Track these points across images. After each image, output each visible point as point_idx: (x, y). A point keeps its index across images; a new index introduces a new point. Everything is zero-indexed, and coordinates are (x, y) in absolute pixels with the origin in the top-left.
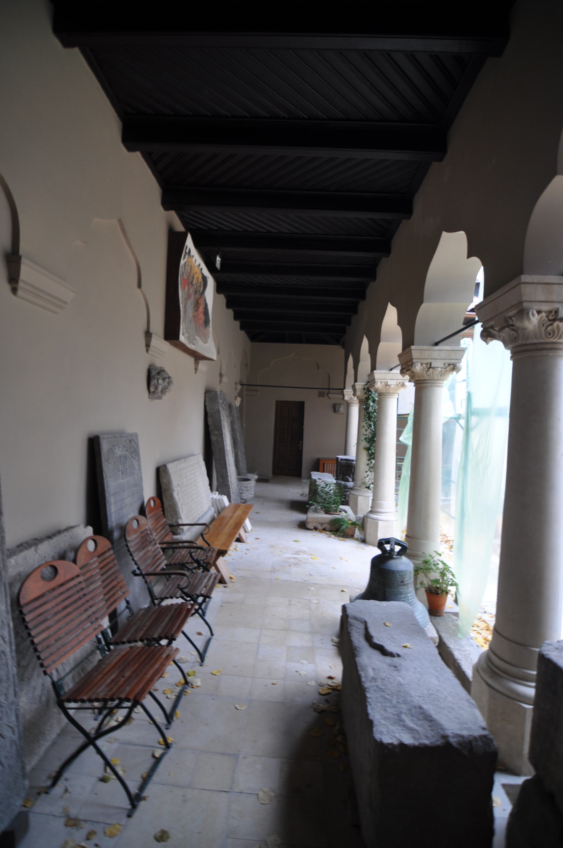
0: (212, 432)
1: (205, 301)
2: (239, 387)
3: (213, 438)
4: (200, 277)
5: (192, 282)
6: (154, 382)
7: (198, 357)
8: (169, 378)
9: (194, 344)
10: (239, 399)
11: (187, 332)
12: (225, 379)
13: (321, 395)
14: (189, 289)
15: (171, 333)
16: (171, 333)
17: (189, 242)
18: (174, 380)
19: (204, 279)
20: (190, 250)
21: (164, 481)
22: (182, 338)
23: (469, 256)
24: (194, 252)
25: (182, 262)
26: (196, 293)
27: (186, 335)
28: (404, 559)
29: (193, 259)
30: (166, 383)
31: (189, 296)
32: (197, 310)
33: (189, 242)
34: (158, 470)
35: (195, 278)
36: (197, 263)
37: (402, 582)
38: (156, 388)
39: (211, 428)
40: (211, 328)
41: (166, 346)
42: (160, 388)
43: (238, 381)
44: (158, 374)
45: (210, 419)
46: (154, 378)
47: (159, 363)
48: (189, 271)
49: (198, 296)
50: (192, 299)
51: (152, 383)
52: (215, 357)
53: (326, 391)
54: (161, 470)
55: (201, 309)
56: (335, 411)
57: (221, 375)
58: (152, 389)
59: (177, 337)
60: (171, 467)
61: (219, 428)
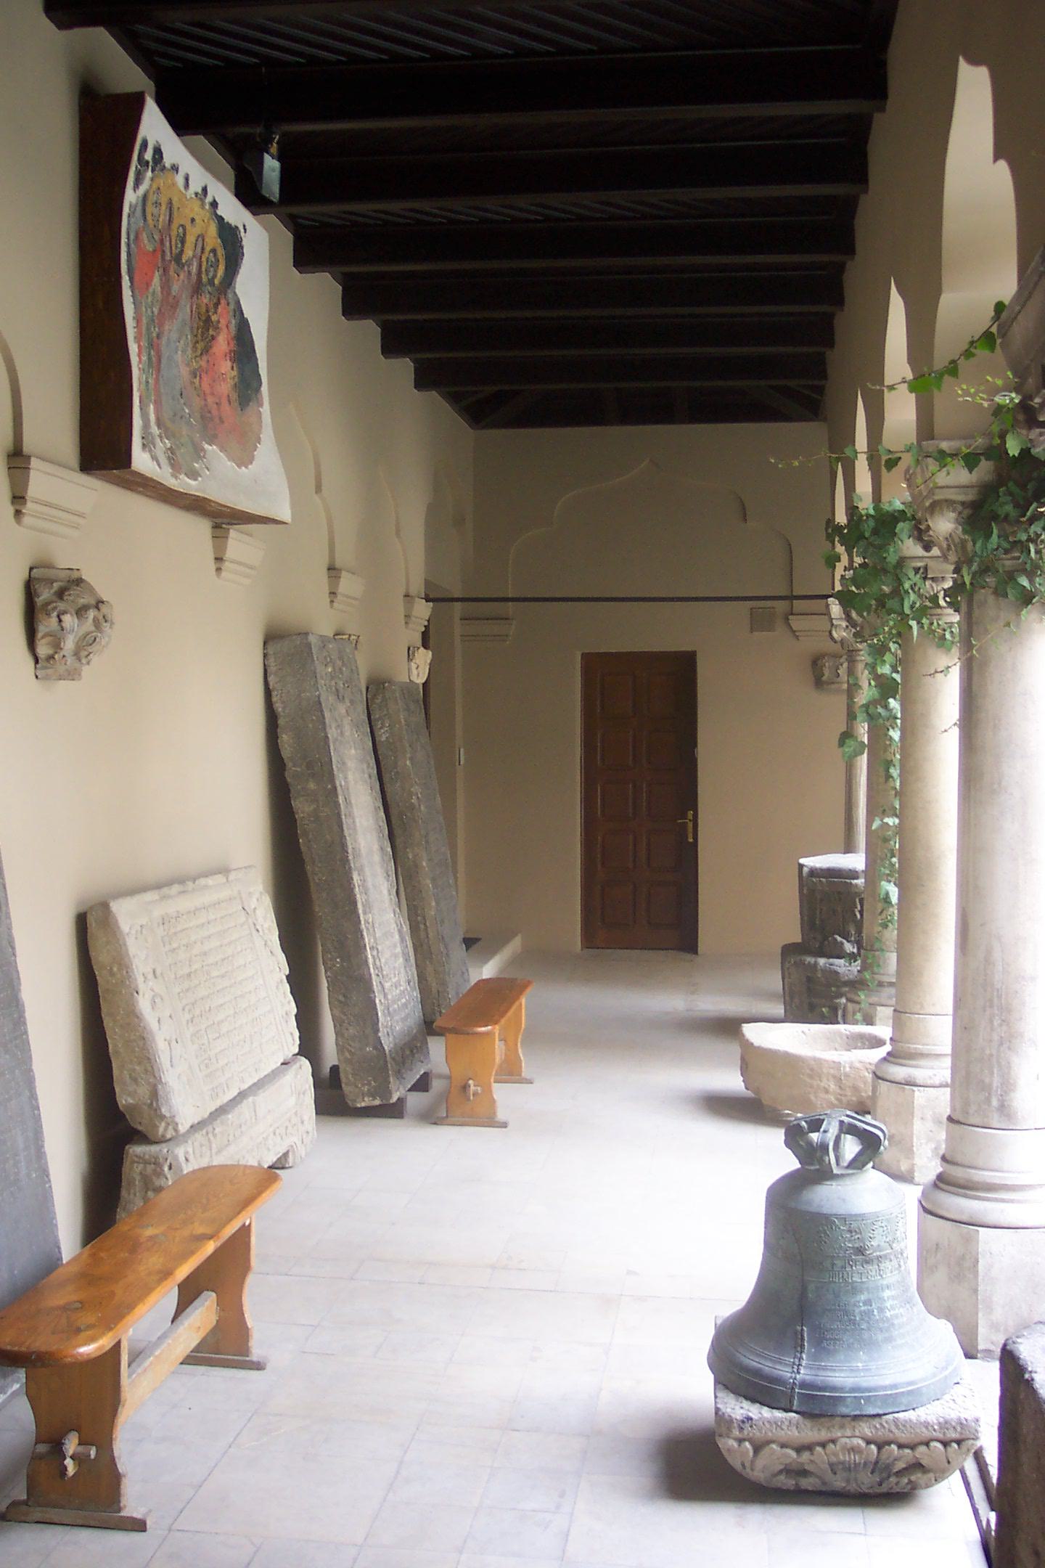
0: (295, 787)
1: (239, 310)
2: (423, 610)
3: (302, 807)
4: (213, 230)
5: (178, 258)
6: (47, 625)
7: (223, 519)
8: (99, 603)
9: (193, 475)
10: (424, 657)
11: (167, 433)
12: (347, 584)
13: (760, 622)
14: (166, 285)
15: (103, 447)
16: (103, 447)
17: (153, 125)
18: (117, 610)
19: (230, 237)
20: (158, 152)
21: (100, 957)
22: (141, 460)
23: (996, 160)
24: (175, 149)
25: (131, 196)
26: (197, 289)
27: (161, 446)
28: (871, 1177)
29: (178, 171)
30: (88, 625)
31: (170, 304)
32: (206, 350)
33: (153, 125)
34: (82, 922)
35: (190, 239)
36: (195, 187)
37: (860, 1251)
38: (57, 646)
39: (292, 770)
40: (266, 409)
41: (92, 493)
42: (69, 644)
43: (418, 587)
44: (60, 594)
45: (285, 739)
46: (50, 604)
47: (66, 558)
48: (163, 219)
49: (205, 299)
50: (185, 311)
51: (41, 630)
52: (285, 514)
53: (781, 606)
54: (91, 920)
55: (223, 343)
56: (819, 683)
57: (333, 570)
58: (43, 650)
59: (124, 459)
60: (126, 913)
61: (322, 770)
